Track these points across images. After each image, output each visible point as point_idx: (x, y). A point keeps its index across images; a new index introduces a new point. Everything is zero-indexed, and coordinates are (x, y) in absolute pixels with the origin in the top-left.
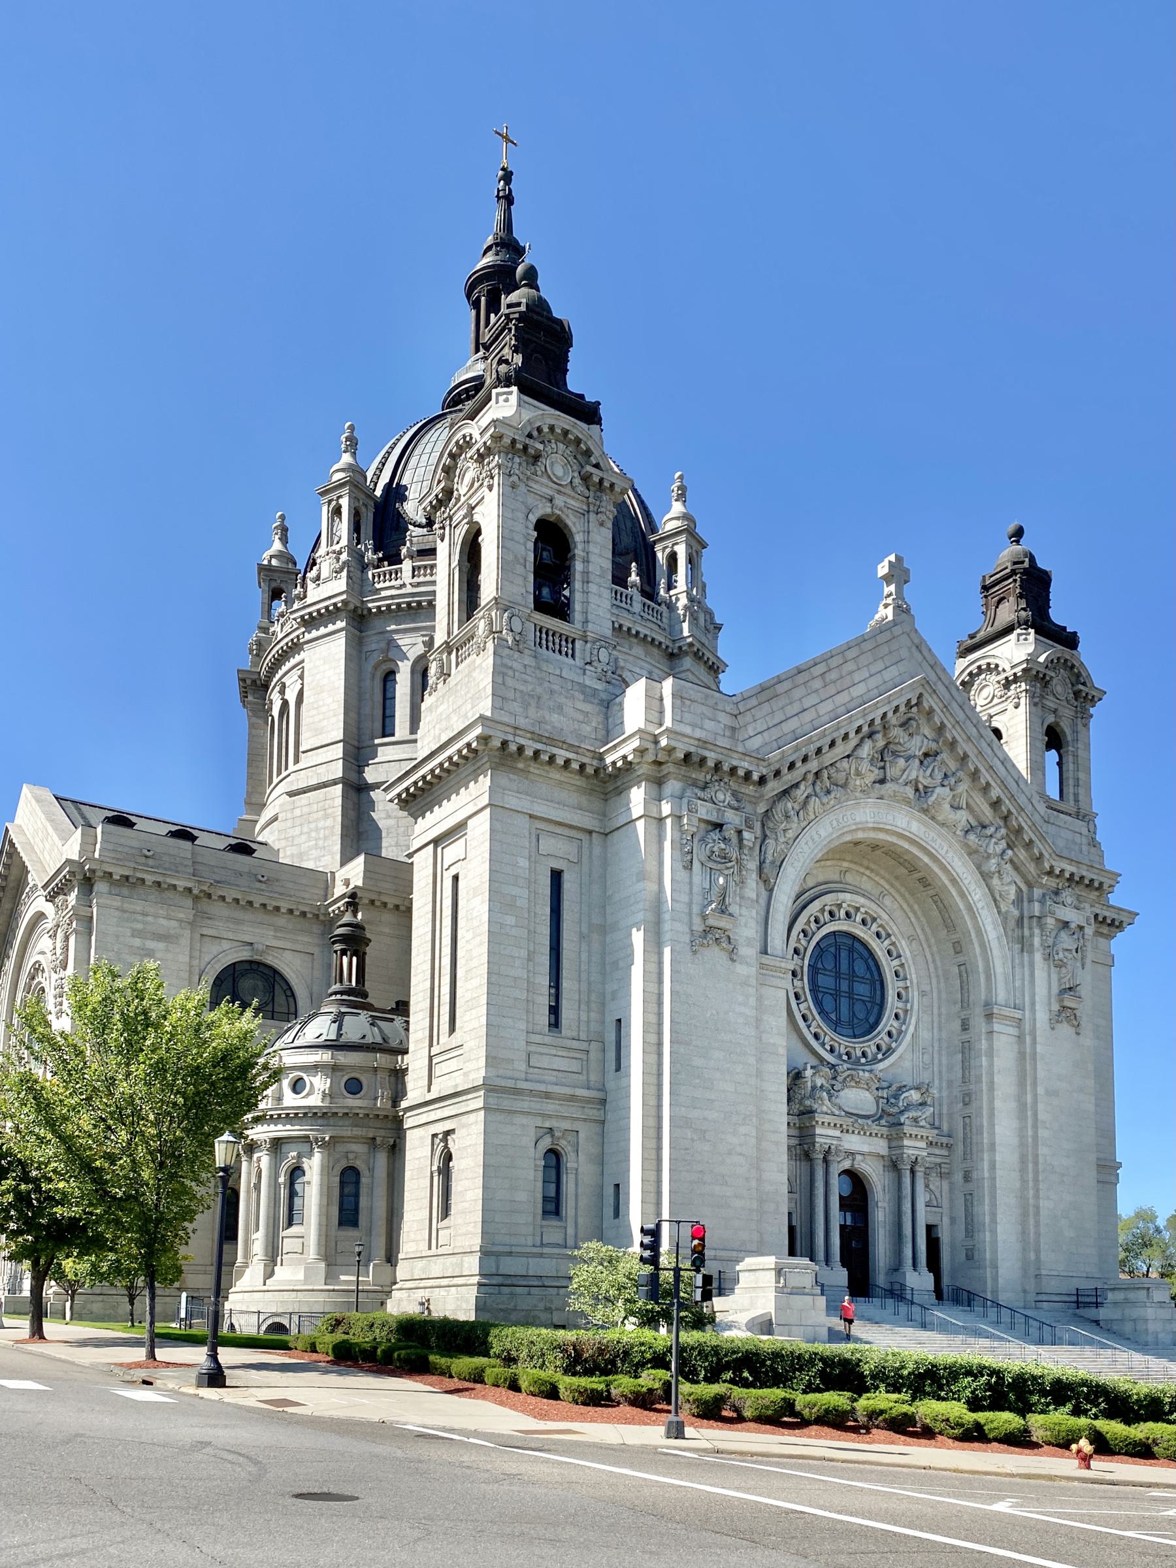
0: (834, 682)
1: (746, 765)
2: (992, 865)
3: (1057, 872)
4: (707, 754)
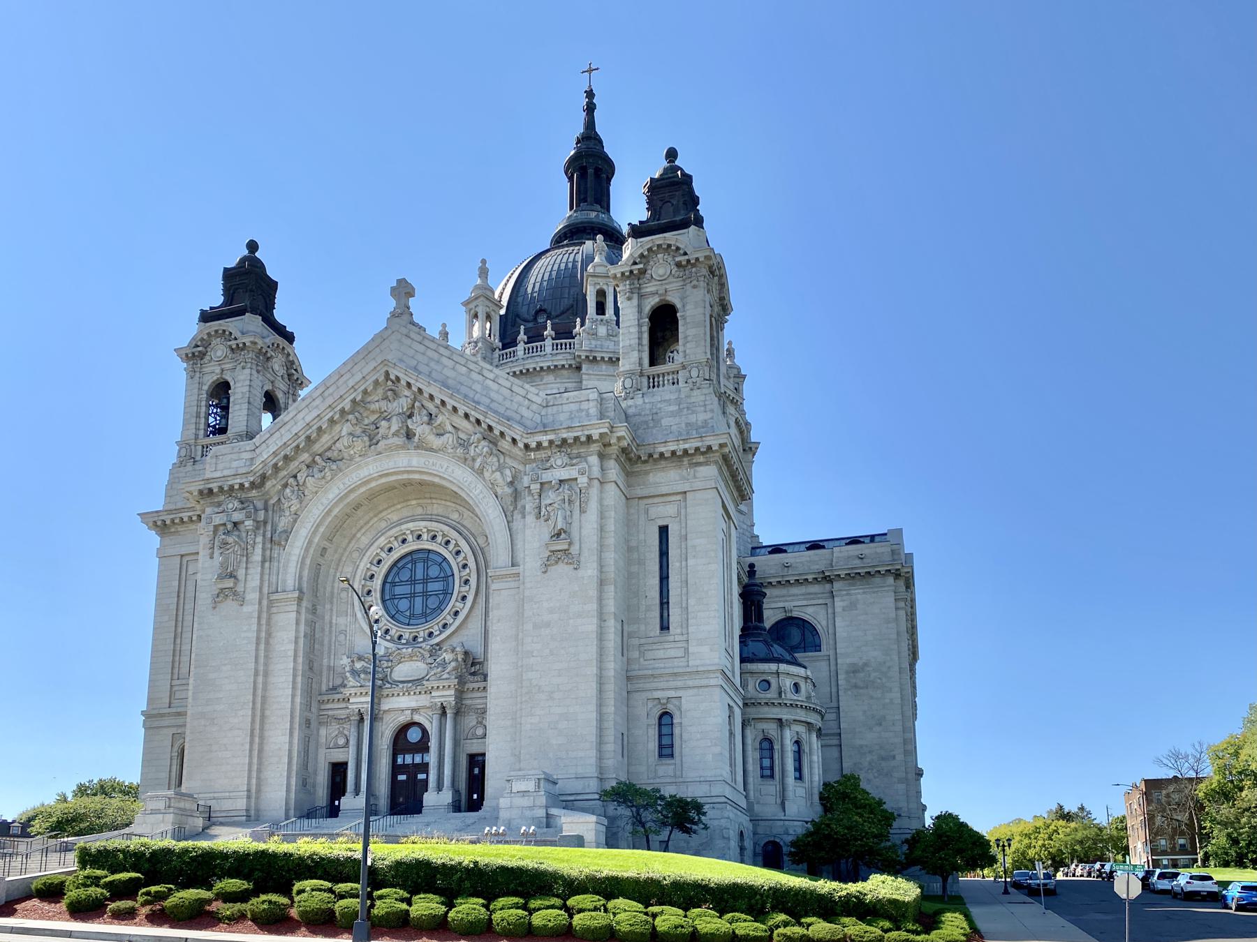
0: (332, 394)
1: (239, 481)
2: (477, 465)
3: (533, 445)
4: (211, 486)
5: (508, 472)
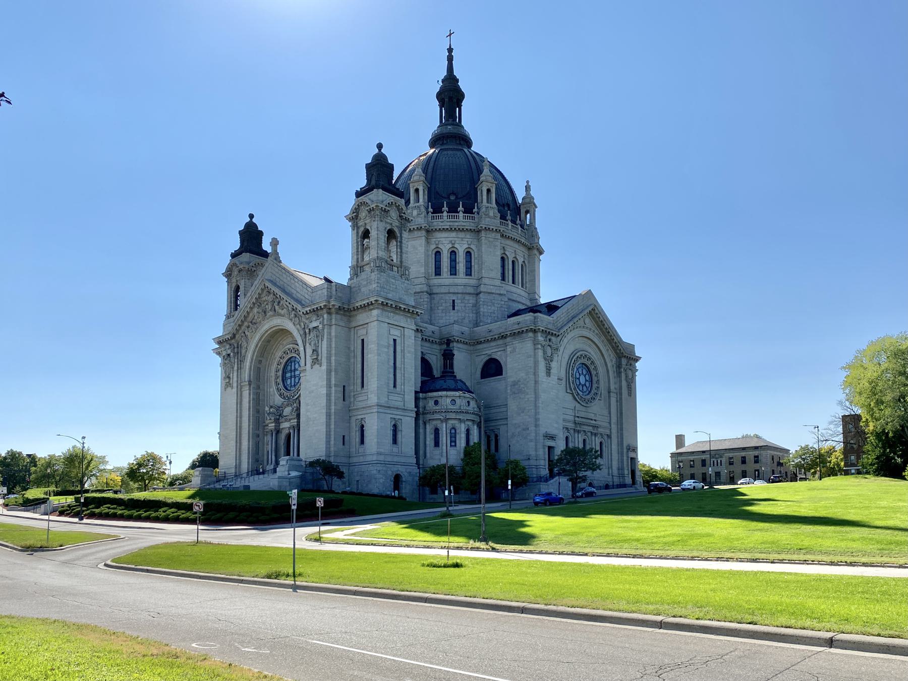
3: (305, 313)
5: (302, 324)
